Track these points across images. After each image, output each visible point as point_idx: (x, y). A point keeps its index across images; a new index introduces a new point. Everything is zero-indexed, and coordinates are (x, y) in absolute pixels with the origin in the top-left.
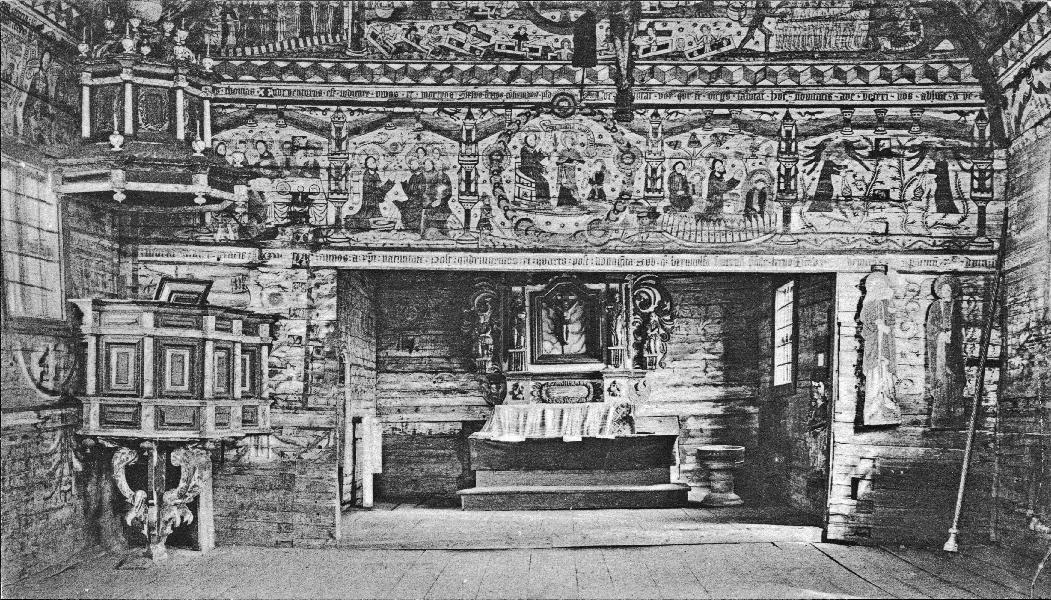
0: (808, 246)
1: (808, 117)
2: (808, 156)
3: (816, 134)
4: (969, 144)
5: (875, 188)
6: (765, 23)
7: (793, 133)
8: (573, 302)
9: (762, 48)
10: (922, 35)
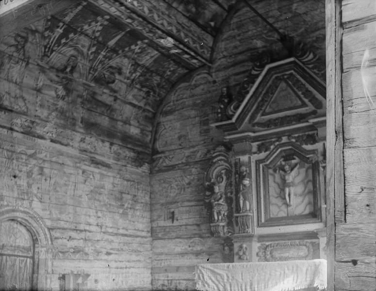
8: (296, 165)
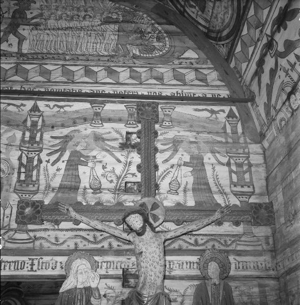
0: (46, 245)
1: (56, 109)
2: (53, 146)
3: (63, 126)
4: (224, 140)
5: (127, 180)
6: (20, 31)
7: (40, 123)
9: (15, 49)
10: (168, 46)
